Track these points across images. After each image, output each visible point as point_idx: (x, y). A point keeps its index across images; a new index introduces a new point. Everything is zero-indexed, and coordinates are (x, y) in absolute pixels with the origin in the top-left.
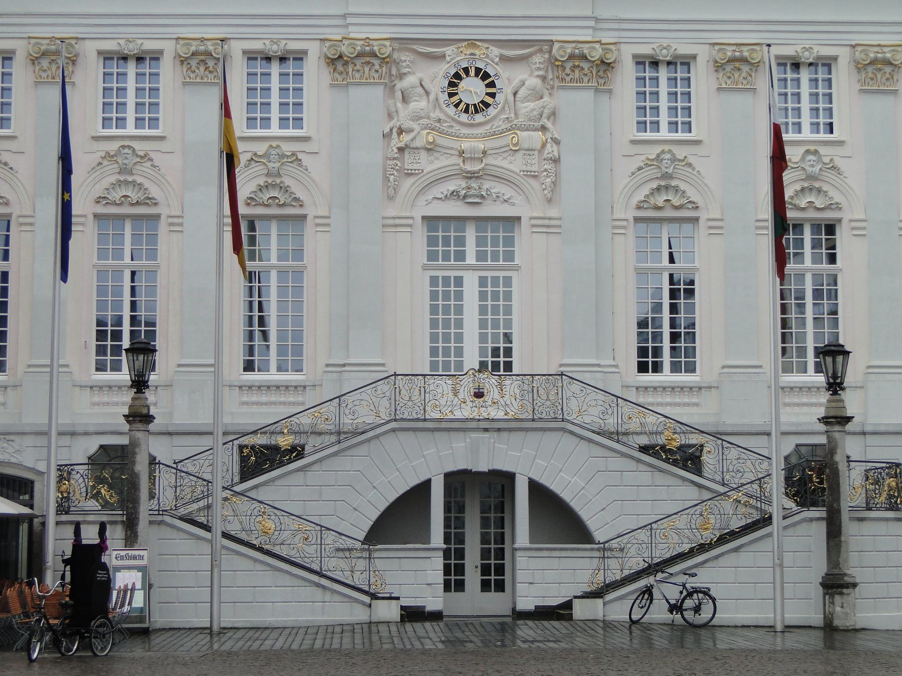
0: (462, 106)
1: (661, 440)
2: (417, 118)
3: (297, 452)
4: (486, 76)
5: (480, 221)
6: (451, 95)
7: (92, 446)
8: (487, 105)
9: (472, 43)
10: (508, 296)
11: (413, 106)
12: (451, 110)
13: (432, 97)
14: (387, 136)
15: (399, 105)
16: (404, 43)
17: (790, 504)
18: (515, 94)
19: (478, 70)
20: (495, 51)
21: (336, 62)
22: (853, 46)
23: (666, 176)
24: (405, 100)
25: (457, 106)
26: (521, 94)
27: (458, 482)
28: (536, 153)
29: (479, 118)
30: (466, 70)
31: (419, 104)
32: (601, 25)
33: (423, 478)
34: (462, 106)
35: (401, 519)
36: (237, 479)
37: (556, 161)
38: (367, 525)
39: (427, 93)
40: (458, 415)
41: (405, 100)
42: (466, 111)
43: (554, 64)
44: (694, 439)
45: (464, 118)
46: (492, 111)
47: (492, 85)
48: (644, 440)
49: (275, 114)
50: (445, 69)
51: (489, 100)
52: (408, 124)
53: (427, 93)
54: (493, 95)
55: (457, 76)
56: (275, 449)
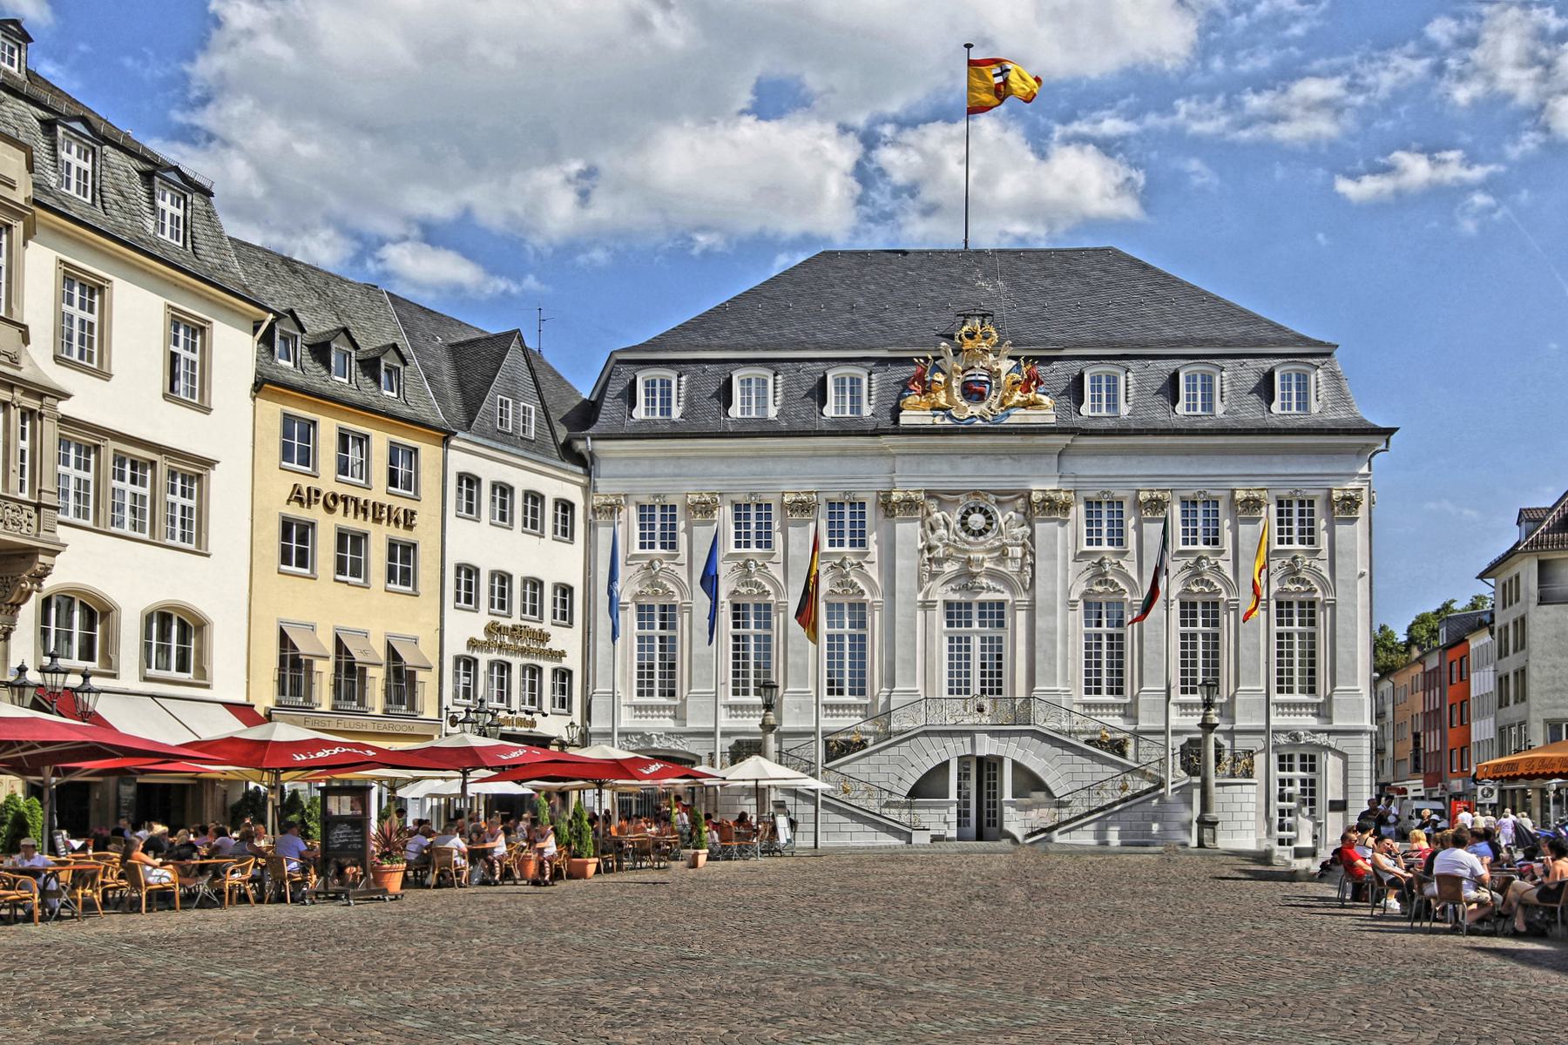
1: (1098, 737)
2: (941, 539)
3: (862, 744)
5: (982, 605)
9: (976, 493)
12: (963, 535)
14: (922, 551)
16: (930, 494)
17: (1184, 774)
20: (992, 498)
24: (933, 529)
29: (981, 539)
31: (942, 531)
35: (928, 787)
37: (1033, 566)
40: (966, 721)
41: (933, 529)
43: (1029, 504)
44: (1119, 736)
45: (971, 539)
48: (1087, 737)
49: (847, 539)
52: (934, 543)
56: (849, 742)
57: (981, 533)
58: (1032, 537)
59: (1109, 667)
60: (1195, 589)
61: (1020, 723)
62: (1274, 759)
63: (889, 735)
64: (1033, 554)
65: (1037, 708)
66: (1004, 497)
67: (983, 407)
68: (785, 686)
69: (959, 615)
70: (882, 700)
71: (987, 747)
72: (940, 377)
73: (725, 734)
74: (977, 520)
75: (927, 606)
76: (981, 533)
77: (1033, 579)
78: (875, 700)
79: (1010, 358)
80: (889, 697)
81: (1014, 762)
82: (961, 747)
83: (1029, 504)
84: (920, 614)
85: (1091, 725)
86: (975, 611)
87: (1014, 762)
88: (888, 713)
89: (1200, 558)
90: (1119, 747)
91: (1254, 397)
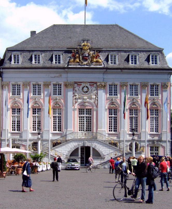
0: (84, 92)
1: (111, 142)
4: (87, 87)
6: (82, 90)
7: (32, 142)
8: (88, 92)
10: (91, 120)
11: (77, 92)
13: (80, 90)
15: (75, 92)
16: (76, 83)
18: (92, 90)
19: (86, 86)
20: (89, 84)
21: (66, 86)
22: (141, 83)
23: (113, 102)
24: (76, 91)
25: (83, 92)
26: (92, 90)
27: (82, 148)
28: (95, 99)
29: (86, 93)
30: (85, 86)
32: (104, 80)
33: (78, 147)
34: (84, 92)
35: (74, 153)
36: (52, 147)
37: (97, 100)
38: (70, 154)
39: (79, 90)
42: (85, 92)
45: (84, 93)
46: (88, 93)
47: (88, 89)
50: (82, 86)
51: (88, 91)
53: (79, 90)
54: (88, 90)
55: (83, 87)
57: (86, 92)
58: (97, 93)
59: (114, 125)
60: (133, 106)
61: (95, 139)
62: (149, 148)
63: (66, 141)
64: (97, 97)
65: (98, 134)
66: (92, 84)
67: (87, 62)
68: (44, 129)
69: (82, 112)
70: (65, 132)
71: (87, 144)
72: (77, 55)
73: (30, 140)
74: (85, 89)
75: (74, 110)
76: (86, 92)
77: (97, 104)
78: (63, 132)
79: (93, 51)
80: (66, 132)
81: (93, 148)
82: (81, 144)
83: (97, 85)
84: (73, 112)
85: (109, 139)
86: (85, 111)
87: (93, 148)
88: (66, 135)
89: (134, 99)
90: (115, 145)
91: (146, 62)
